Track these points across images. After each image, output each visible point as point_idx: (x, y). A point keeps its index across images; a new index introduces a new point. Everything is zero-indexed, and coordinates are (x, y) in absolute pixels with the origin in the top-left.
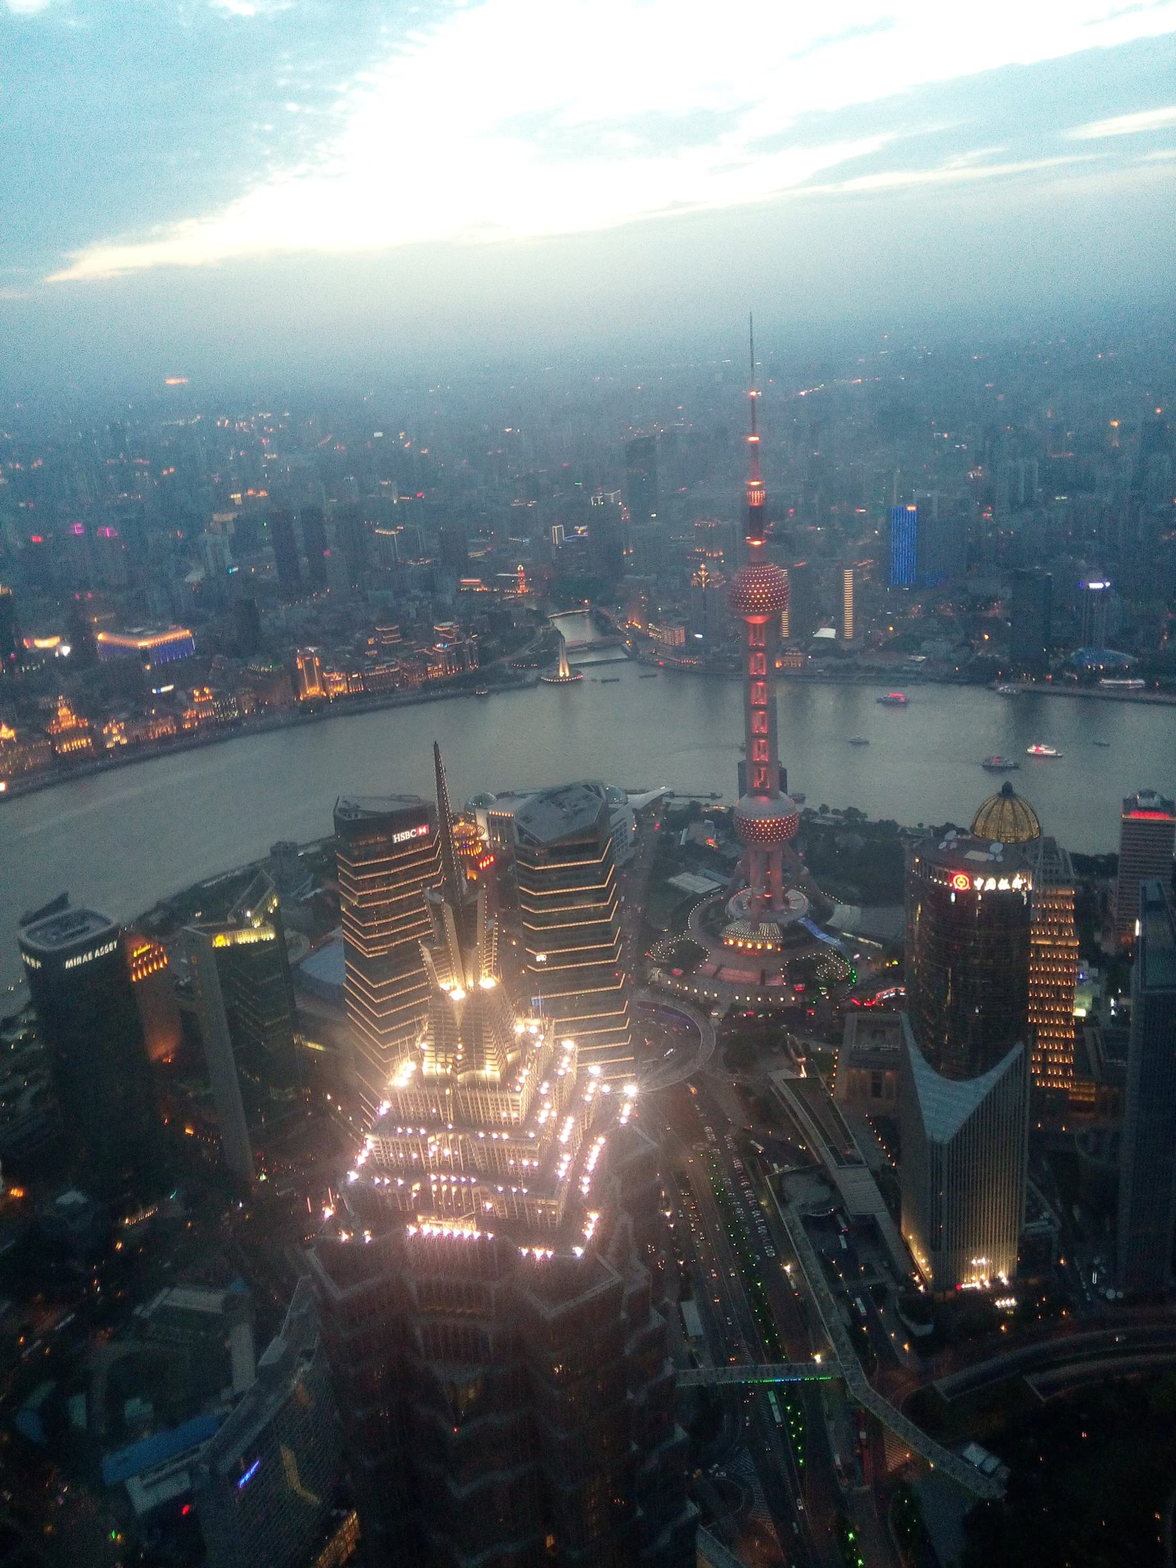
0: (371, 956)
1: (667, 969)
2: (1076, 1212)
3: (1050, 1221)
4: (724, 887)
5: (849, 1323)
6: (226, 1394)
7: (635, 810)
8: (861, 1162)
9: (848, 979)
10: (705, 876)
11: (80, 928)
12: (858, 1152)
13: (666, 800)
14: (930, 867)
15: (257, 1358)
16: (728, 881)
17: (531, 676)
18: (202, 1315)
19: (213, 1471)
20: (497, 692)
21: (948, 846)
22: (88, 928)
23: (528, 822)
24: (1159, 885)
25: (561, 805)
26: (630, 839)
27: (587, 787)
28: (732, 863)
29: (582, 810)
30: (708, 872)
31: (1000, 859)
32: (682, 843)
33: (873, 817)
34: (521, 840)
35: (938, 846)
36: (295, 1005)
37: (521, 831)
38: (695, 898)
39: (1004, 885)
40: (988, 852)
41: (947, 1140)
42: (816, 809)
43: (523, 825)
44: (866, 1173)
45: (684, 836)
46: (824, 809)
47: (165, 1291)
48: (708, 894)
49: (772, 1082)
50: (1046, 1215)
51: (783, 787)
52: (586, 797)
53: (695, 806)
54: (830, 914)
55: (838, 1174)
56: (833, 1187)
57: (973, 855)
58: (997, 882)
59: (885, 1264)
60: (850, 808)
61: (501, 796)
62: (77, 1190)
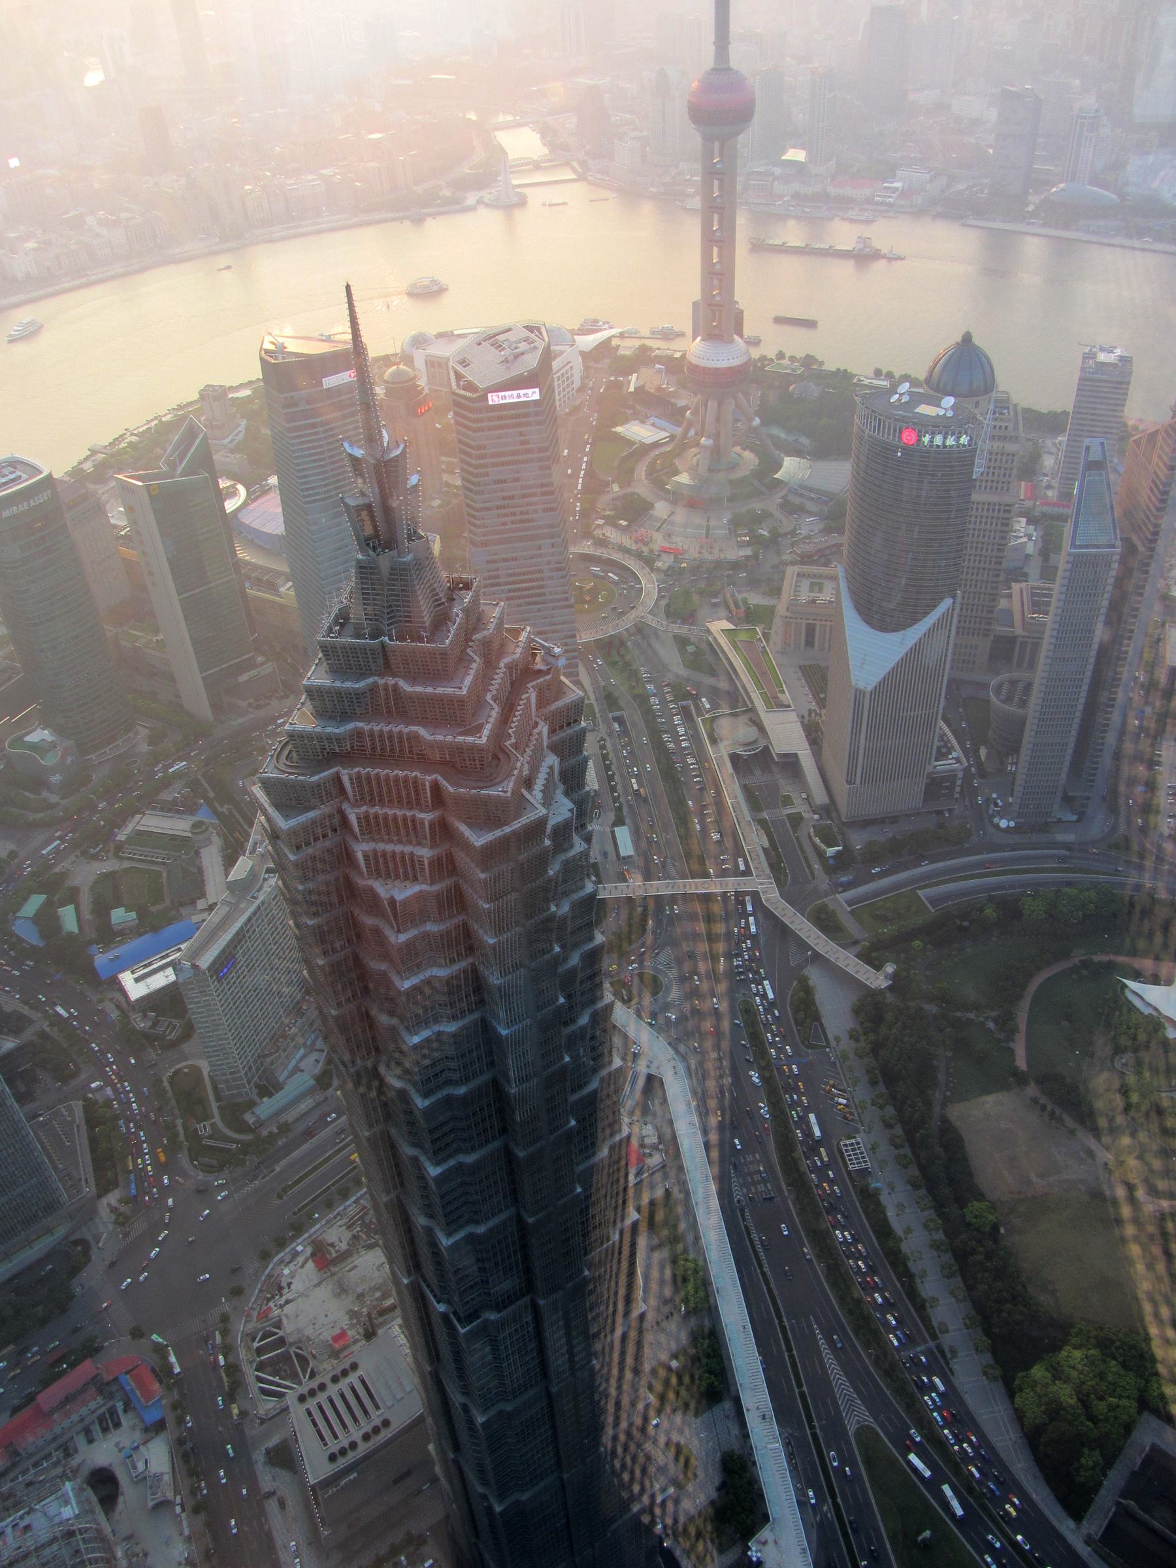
1: (611, 522)
2: (983, 752)
3: (958, 760)
4: (672, 438)
5: (767, 845)
6: (201, 904)
7: (582, 353)
9: (793, 533)
10: (653, 425)
11: (12, 476)
12: (786, 697)
13: (615, 342)
15: (227, 875)
16: (678, 431)
17: (471, 199)
18: (173, 838)
19: (195, 967)
20: (433, 215)
21: (899, 400)
22: (20, 477)
23: (465, 367)
24: (1102, 444)
25: (499, 347)
26: (577, 384)
27: (530, 329)
29: (523, 354)
30: (657, 421)
31: (950, 414)
32: (632, 389)
33: (830, 366)
34: (458, 385)
37: (459, 376)
38: (645, 449)
39: (950, 441)
40: (939, 406)
41: (869, 688)
42: (772, 354)
43: (460, 369)
44: (793, 716)
45: (633, 382)
46: (781, 355)
47: (138, 817)
48: (656, 445)
49: (708, 631)
50: (954, 754)
51: (739, 330)
52: (526, 340)
53: (644, 349)
54: (779, 466)
55: (769, 719)
56: (761, 729)
57: (925, 409)
58: (945, 438)
60: (808, 356)
61: (440, 335)
62: (43, 729)
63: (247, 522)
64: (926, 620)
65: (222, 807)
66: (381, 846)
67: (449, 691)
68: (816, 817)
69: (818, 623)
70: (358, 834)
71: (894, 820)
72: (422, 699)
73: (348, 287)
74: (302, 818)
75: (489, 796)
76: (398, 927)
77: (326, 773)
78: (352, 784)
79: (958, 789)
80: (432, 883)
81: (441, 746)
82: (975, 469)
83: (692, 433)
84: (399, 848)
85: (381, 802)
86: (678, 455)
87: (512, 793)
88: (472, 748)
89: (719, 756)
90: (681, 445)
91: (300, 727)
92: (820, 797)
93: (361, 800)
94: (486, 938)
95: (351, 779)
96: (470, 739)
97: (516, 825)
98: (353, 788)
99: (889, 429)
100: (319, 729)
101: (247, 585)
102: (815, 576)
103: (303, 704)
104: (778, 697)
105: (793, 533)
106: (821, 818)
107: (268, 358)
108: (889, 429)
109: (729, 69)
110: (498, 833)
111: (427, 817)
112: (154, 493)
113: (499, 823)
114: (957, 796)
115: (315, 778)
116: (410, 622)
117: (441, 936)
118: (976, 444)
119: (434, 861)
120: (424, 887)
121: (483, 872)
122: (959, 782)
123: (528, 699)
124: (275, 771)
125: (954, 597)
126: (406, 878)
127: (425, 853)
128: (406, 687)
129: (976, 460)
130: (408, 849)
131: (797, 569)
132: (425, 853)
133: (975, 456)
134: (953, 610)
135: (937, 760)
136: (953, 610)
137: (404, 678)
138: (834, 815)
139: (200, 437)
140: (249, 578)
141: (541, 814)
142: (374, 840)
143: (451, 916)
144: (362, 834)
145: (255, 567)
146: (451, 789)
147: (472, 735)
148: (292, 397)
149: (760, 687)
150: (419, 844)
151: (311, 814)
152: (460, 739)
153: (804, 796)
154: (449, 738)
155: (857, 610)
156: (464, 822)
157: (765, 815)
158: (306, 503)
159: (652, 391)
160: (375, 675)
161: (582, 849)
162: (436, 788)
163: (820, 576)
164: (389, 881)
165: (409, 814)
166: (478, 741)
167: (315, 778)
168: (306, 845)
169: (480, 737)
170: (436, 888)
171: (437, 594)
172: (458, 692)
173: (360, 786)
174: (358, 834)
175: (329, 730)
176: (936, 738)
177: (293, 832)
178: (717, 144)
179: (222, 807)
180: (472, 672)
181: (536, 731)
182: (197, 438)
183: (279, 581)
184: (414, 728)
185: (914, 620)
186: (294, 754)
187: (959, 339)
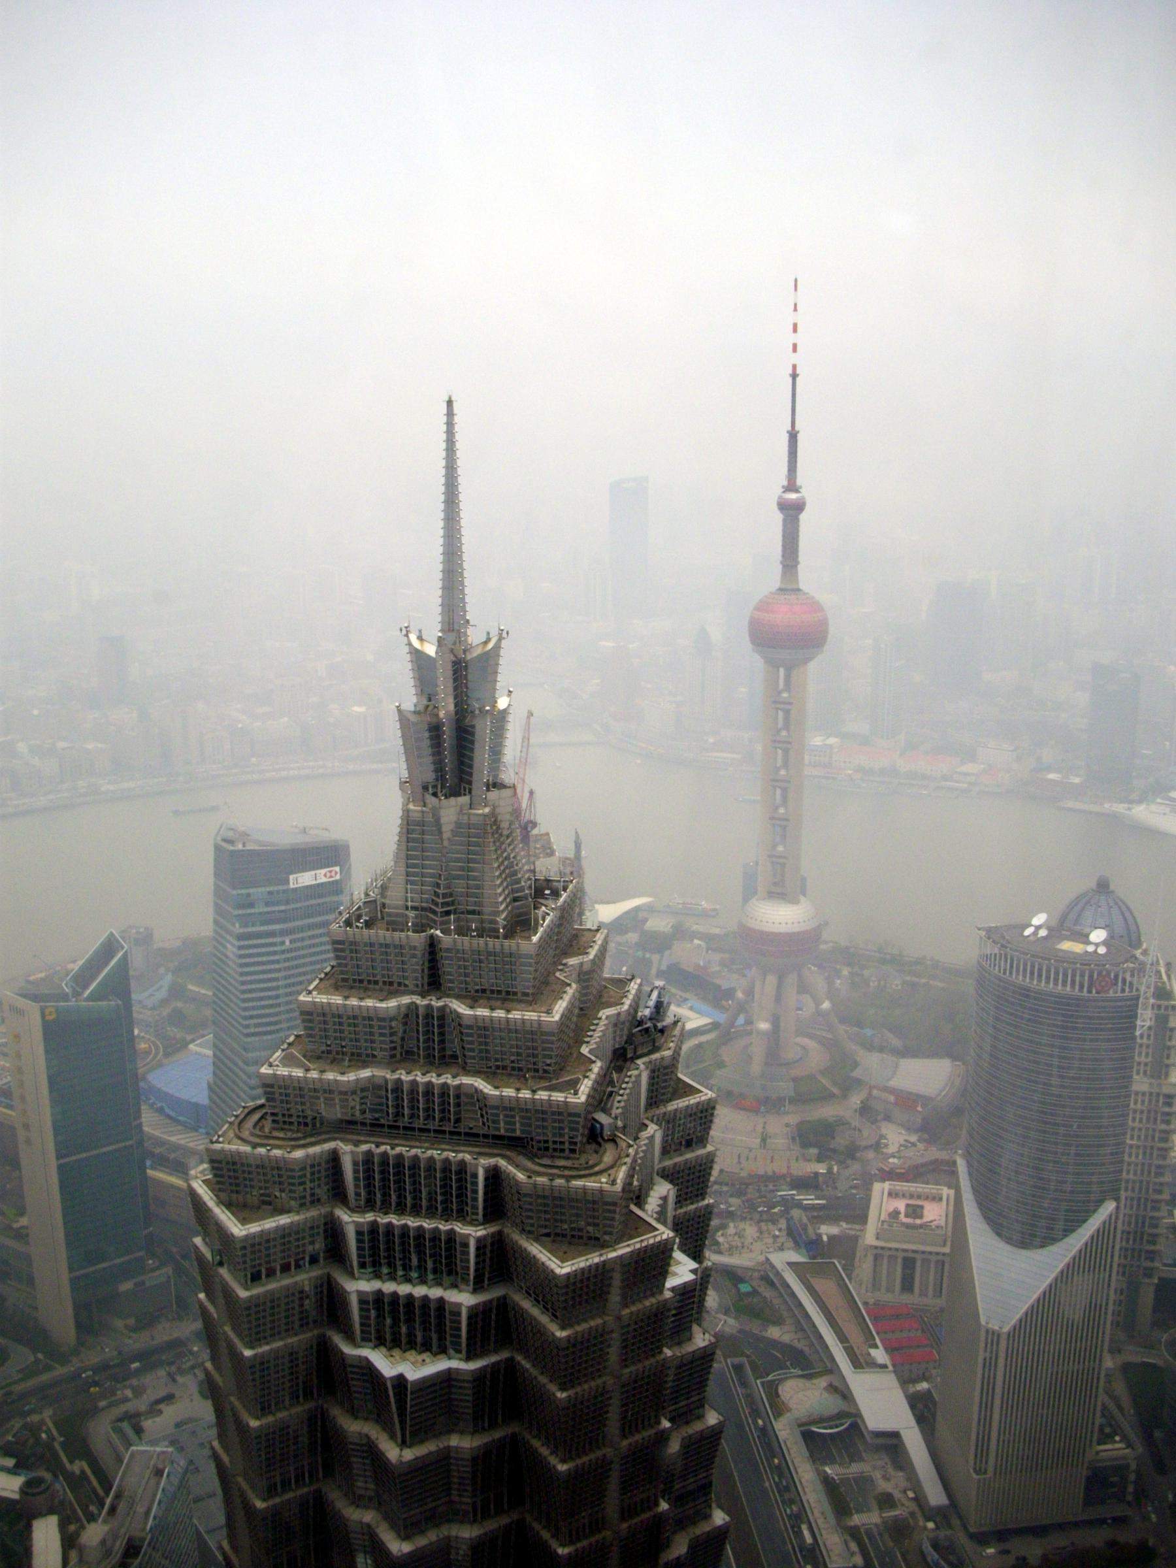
0: (249, 1039)
2: (1157, 1434)
4: (715, 1026)
8: (885, 1366)
10: (691, 1008)
13: (641, 915)
14: (1012, 960)
21: (1035, 933)
28: (729, 993)
31: (1102, 950)
32: (664, 967)
35: (1023, 931)
36: (139, 1117)
40: (1089, 943)
41: (1005, 1330)
59: (911, 1494)
63: (159, 1086)
64: (1080, 1231)
65: (71, 1462)
66: (389, 1287)
67: (531, 1016)
68: (931, 1525)
69: (919, 1257)
70: (355, 1264)
71: (1039, 1531)
72: (484, 1029)
73: (450, 403)
74: (270, 1224)
75: (584, 1189)
76: (404, 1436)
77: (316, 1149)
78: (356, 1171)
79: (1131, 1488)
80: (468, 1359)
81: (510, 1108)
82: (1139, 1023)
83: (741, 1020)
84: (419, 1291)
85: (401, 1210)
86: (725, 1044)
87: (624, 1190)
88: (563, 1113)
89: (784, 1430)
90: (725, 1034)
91: (283, 1071)
92: (936, 1496)
93: (370, 1205)
94: (553, 1460)
95: (355, 1163)
96: (558, 1096)
97: (623, 1250)
98: (356, 1179)
99: (1025, 970)
100: (314, 1074)
101: (148, 1163)
102: (911, 1197)
103: (289, 1044)
104: (869, 1354)
105: (877, 1146)
106: (937, 1528)
107: (223, 844)
108: (1025, 970)
109: (799, 590)
110: (595, 1258)
111: (472, 1233)
112: (48, 1018)
113: (598, 1243)
114: (1129, 1498)
115: (299, 1154)
116: (479, 913)
117: (474, 1459)
118: (1137, 990)
119: (476, 1315)
120: (455, 1364)
121: (563, 1328)
122: (1132, 1477)
123: (640, 1075)
124: (236, 1140)
125: (1117, 1199)
126: (426, 1347)
127: (463, 1299)
128: (460, 1008)
129: (1139, 1011)
130: (435, 1293)
131: (887, 1186)
132: (463, 1299)
133: (1137, 1005)
134: (1117, 1218)
135: (1099, 1443)
136: (1117, 1218)
137: (458, 997)
138: (956, 1522)
139: (120, 954)
140: (152, 1155)
141: (665, 1237)
142: (377, 1276)
143: (493, 1425)
144: (362, 1265)
145: (162, 1143)
146: (521, 1176)
147: (560, 1091)
148: (249, 895)
149: (842, 1338)
150: (454, 1286)
151: (284, 1220)
152: (543, 1095)
153: (911, 1494)
154: (525, 1094)
155: (985, 1217)
156: (537, 1240)
157: (856, 1519)
158: (248, 1035)
159: (691, 970)
160: (413, 993)
161: (706, 1343)
162: (495, 1177)
163: (919, 1197)
164: (397, 1352)
165: (444, 1227)
166: (572, 1099)
167: (299, 1154)
168: (268, 1276)
169: (576, 1093)
170: (473, 1366)
171: (518, 882)
172: (545, 1018)
173: (369, 1177)
174: (355, 1264)
175: (330, 1076)
176: (1098, 1414)
177: (253, 1244)
178: (782, 670)
179: (71, 1462)
180: (567, 997)
181: (644, 1134)
182: (113, 957)
183: (192, 1162)
184: (466, 1080)
185: (1068, 1231)
186: (268, 1125)
187: (1093, 885)
